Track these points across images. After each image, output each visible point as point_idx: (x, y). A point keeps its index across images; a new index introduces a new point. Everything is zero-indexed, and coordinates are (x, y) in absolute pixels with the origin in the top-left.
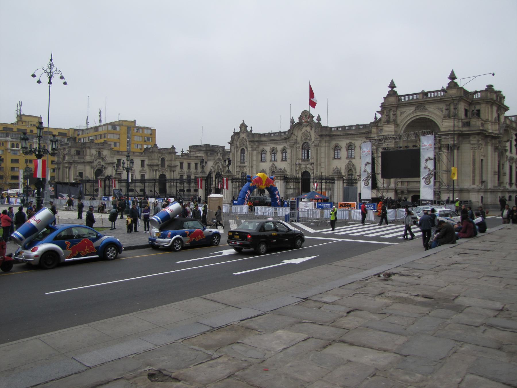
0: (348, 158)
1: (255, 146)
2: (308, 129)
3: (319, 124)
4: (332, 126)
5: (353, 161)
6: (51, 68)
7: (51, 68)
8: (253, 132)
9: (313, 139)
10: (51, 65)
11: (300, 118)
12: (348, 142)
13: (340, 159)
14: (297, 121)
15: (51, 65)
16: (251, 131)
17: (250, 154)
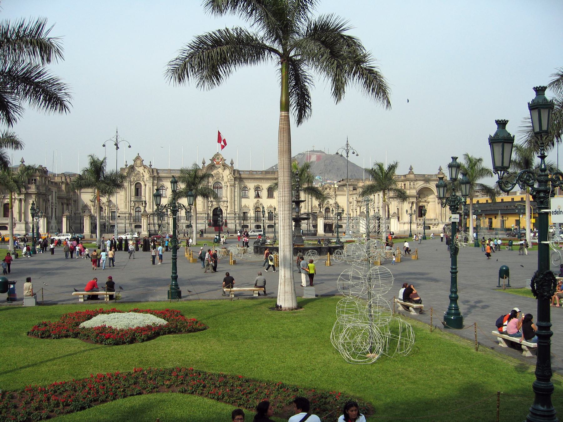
0: (256, 197)
1: (156, 182)
2: (220, 170)
3: (232, 167)
4: (240, 170)
5: (260, 200)
6: (347, 147)
7: (347, 147)
8: (152, 167)
9: (225, 179)
10: (347, 144)
11: (213, 160)
12: (256, 184)
13: (248, 198)
14: (208, 162)
15: (347, 144)
16: (151, 166)
17: (150, 188)
